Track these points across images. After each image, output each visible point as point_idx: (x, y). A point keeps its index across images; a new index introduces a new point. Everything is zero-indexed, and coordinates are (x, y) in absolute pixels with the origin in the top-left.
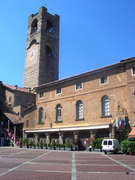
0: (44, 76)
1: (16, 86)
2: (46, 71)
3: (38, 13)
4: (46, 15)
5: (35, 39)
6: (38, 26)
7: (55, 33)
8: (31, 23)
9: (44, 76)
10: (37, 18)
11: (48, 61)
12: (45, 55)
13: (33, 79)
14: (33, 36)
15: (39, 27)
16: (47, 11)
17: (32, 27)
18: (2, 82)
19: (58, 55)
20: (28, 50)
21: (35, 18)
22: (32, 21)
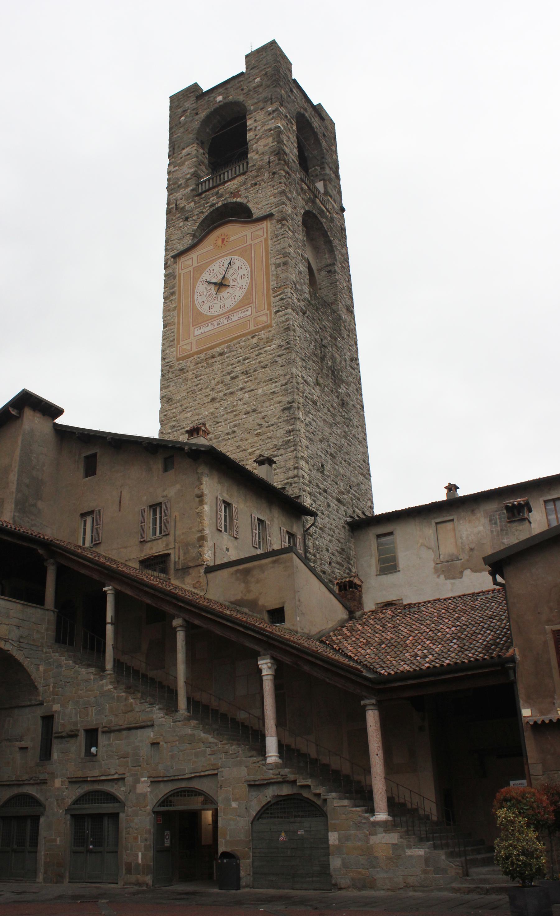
0: (315, 403)
1: (194, 431)
2: (321, 381)
3: (242, 74)
4: (292, 91)
5: (239, 200)
6: (250, 135)
7: (326, 193)
8: (196, 125)
9: (315, 403)
10: (241, 98)
11: (323, 329)
12: (306, 289)
13: (250, 421)
14: (221, 190)
15: (262, 142)
16: (290, 71)
17: (201, 151)
18: (59, 412)
19: (350, 310)
20: (185, 261)
21: (220, 98)
22: (203, 115)
